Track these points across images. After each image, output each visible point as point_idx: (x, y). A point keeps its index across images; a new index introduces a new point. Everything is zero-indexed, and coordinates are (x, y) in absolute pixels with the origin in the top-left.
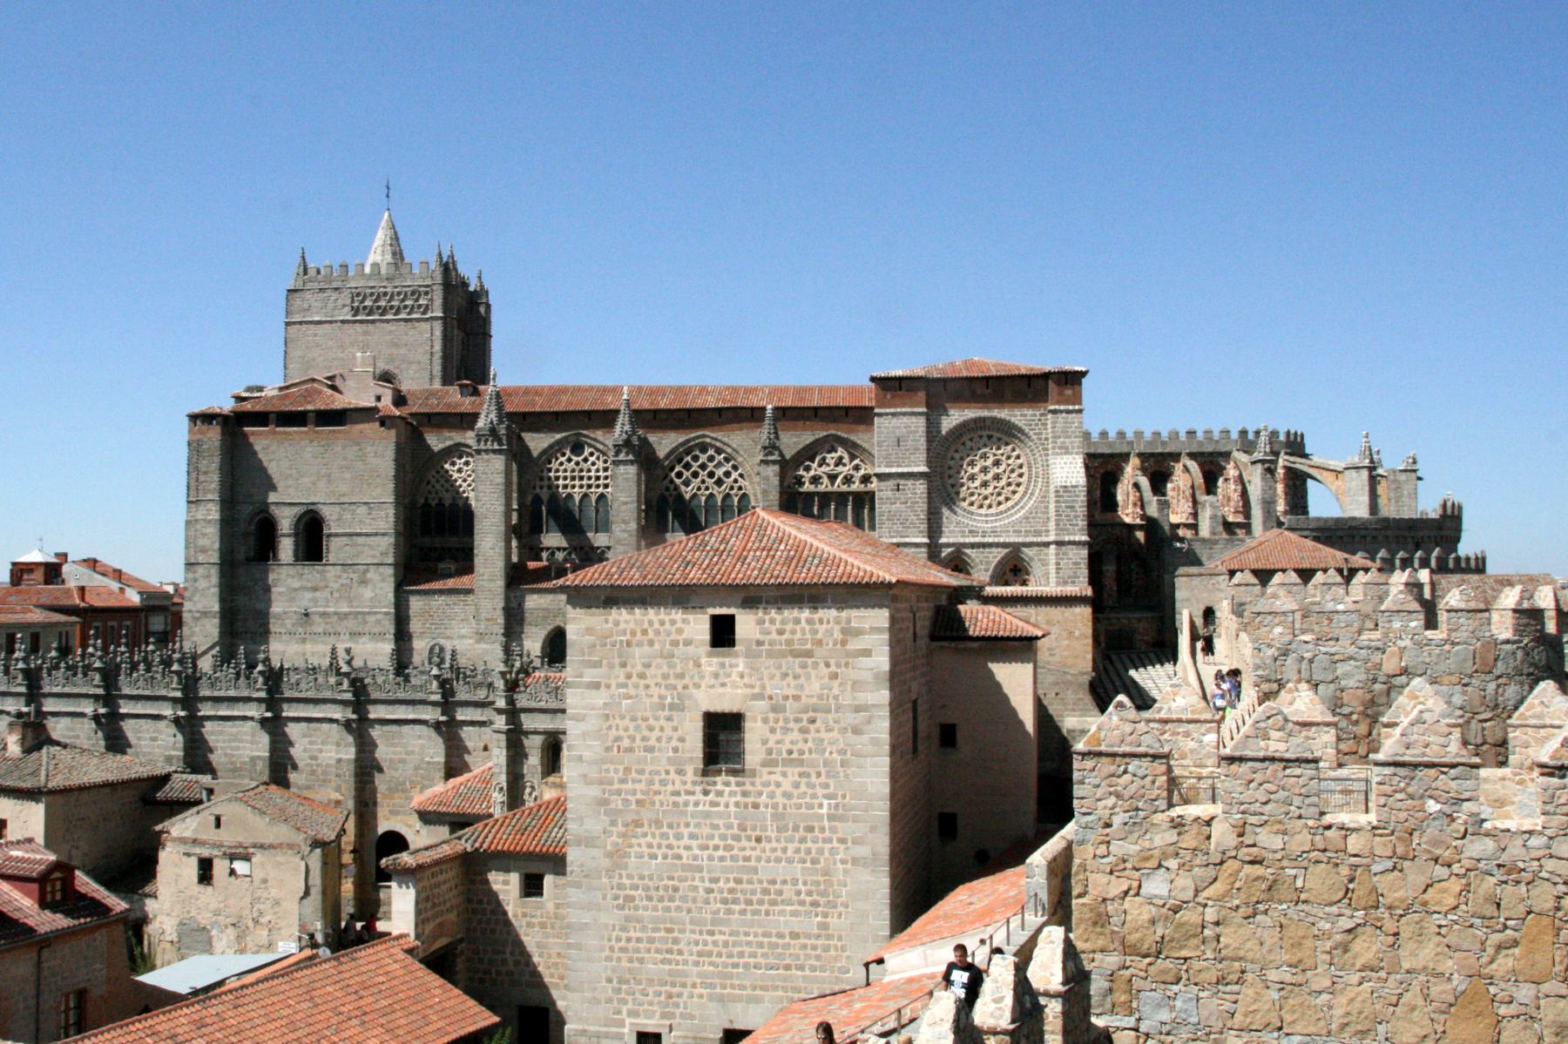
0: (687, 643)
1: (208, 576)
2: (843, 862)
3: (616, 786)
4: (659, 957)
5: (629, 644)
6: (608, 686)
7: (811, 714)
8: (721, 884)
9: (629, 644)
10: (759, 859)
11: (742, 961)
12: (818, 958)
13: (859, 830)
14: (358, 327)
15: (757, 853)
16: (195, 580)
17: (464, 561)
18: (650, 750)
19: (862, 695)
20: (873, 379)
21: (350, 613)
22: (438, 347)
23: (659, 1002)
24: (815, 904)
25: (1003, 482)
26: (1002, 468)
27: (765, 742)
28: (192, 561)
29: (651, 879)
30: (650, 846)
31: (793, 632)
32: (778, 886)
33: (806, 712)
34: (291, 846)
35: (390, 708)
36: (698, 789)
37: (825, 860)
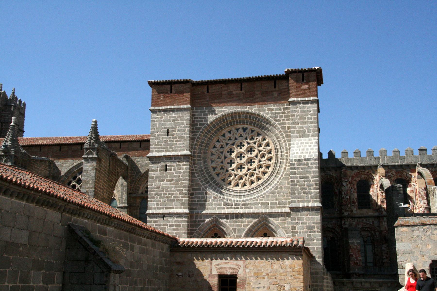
25: (255, 165)
26: (254, 154)
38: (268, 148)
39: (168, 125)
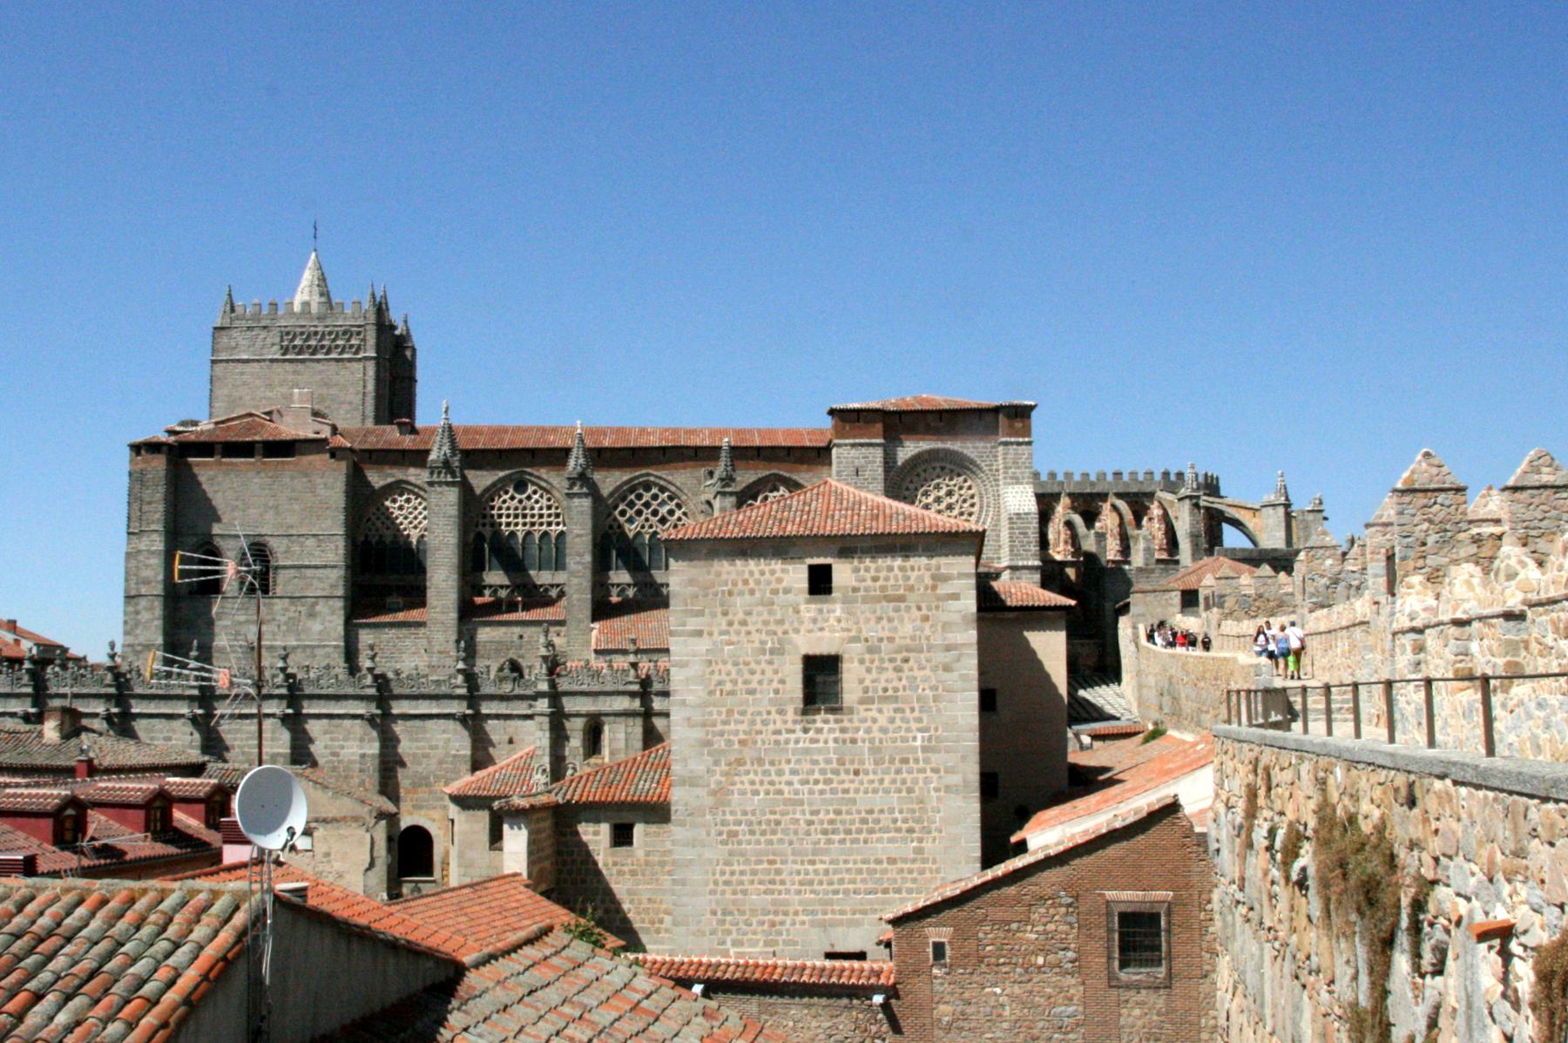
0: (787, 591)
1: (151, 609)
2: (937, 790)
3: (719, 727)
4: (762, 887)
5: (730, 593)
6: (710, 634)
7: (905, 654)
8: (821, 816)
9: (730, 593)
10: (857, 791)
11: (841, 887)
12: (914, 880)
13: (951, 759)
14: (288, 366)
15: (856, 785)
16: (137, 613)
17: (416, 595)
18: (751, 692)
19: (950, 635)
20: (832, 412)
21: (298, 647)
22: (371, 386)
23: (763, 931)
24: (911, 830)
27: (861, 681)
28: (133, 593)
29: (753, 813)
30: (752, 783)
31: (887, 579)
32: (875, 816)
33: (899, 651)
34: (355, 819)
35: (414, 703)
36: (798, 727)
37: (921, 789)
38: (971, 492)
39: (857, 463)
